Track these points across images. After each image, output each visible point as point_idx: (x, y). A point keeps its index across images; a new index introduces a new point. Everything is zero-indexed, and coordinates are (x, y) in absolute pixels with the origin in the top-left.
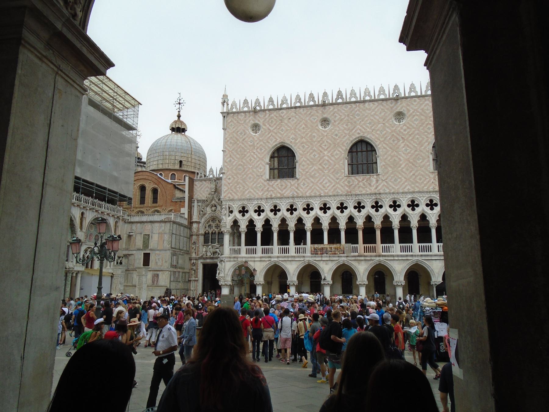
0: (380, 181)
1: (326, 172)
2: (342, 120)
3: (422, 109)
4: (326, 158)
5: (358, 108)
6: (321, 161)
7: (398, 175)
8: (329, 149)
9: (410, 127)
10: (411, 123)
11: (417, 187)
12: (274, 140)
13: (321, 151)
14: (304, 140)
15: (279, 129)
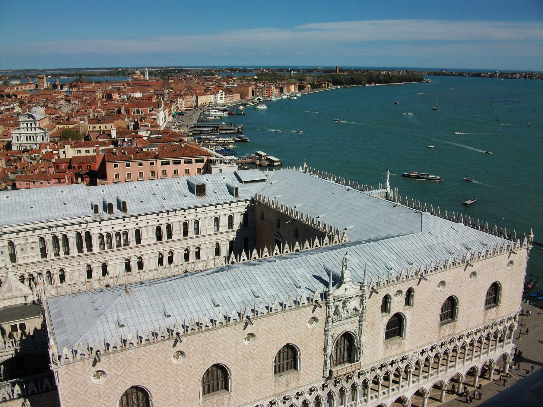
0: (232, 399)
1: (182, 403)
2: (196, 351)
3: (270, 328)
4: (182, 390)
5: (212, 336)
6: (176, 395)
7: (247, 389)
8: (184, 382)
9: (259, 346)
10: (259, 342)
11: (262, 396)
12: (124, 384)
13: (176, 386)
14: (157, 378)
15: (128, 372)
